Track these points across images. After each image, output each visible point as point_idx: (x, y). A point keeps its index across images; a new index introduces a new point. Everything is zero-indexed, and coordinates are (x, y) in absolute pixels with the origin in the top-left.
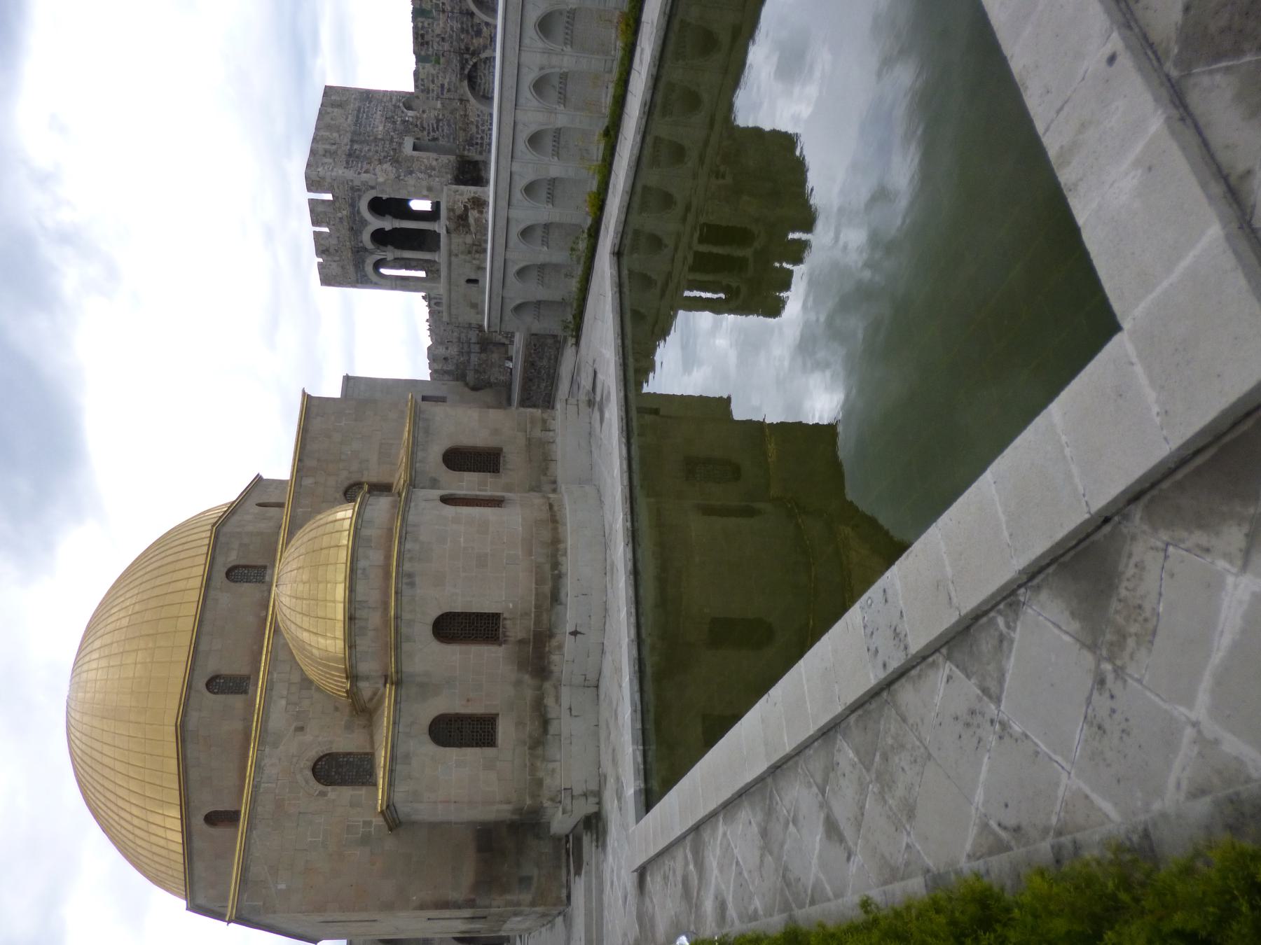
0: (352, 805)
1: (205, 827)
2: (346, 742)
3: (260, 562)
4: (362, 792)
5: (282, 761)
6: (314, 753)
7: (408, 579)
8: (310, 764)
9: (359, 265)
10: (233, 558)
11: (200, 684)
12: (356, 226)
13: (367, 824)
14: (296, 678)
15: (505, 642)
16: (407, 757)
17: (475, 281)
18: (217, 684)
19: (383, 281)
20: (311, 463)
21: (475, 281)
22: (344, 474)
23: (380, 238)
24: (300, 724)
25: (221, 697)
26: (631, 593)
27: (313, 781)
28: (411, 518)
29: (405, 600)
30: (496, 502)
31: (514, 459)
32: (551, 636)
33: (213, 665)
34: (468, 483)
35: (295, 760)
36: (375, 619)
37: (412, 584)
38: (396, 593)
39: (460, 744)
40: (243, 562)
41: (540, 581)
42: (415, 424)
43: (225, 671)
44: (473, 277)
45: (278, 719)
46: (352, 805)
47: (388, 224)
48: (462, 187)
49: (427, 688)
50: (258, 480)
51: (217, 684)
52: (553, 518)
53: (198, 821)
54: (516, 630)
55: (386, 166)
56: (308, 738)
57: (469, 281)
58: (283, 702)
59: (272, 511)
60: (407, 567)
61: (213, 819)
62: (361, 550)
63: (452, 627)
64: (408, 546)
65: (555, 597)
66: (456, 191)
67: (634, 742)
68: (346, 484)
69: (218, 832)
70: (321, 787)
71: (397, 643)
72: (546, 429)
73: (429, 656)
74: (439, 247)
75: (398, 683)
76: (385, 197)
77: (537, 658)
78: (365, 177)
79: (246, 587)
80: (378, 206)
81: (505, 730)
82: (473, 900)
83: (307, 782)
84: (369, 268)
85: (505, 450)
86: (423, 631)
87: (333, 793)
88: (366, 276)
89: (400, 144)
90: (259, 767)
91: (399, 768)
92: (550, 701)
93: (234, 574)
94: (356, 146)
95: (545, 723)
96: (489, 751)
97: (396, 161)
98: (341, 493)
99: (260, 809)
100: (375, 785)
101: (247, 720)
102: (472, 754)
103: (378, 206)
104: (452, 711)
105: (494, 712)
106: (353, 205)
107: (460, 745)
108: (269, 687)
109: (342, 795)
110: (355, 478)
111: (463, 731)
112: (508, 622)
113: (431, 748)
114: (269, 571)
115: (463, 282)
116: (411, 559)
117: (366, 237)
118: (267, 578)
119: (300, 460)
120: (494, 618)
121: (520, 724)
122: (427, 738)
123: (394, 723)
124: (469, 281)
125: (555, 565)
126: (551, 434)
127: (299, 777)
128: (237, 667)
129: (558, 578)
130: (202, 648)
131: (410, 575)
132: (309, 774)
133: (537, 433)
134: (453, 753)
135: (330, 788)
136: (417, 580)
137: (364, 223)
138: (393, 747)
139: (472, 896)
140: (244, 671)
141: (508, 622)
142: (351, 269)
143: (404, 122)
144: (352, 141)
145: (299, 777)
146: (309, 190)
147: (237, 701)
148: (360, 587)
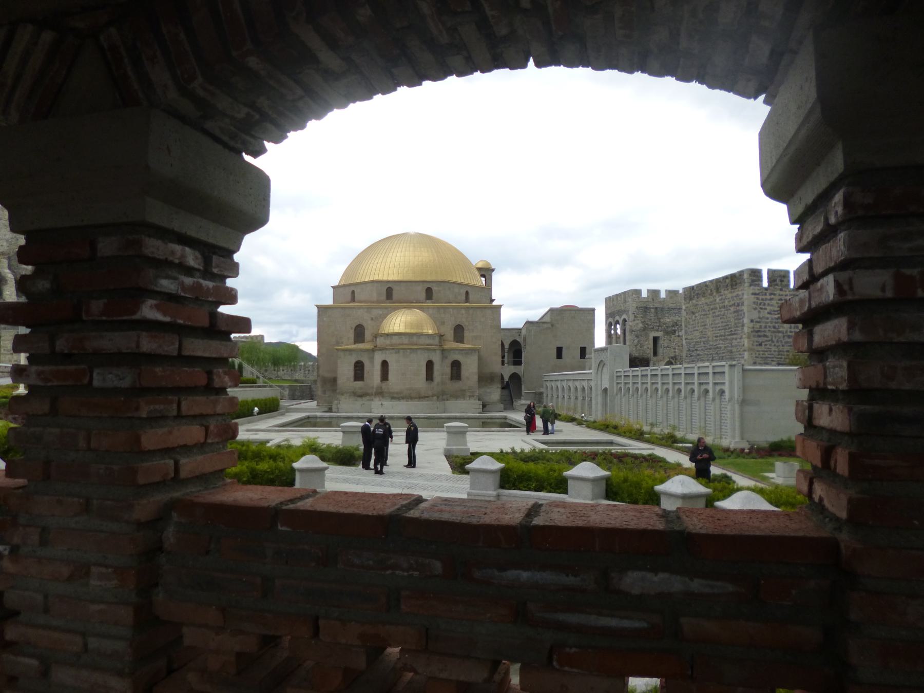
2: (368, 335)
4: (352, 340)
6: (365, 324)
7: (397, 351)
11: (390, 285)
22: (467, 324)
25: (385, 292)
28: (419, 352)
30: (430, 376)
31: (457, 385)
32: (383, 397)
34: (442, 370)
36: (388, 342)
39: (355, 371)
41: (397, 393)
42: (469, 349)
43: (394, 292)
45: (375, 312)
49: (372, 359)
52: (421, 398)
53: (352, 288)
54: (384, 385)
55: (641, 325)
56: (370, 322)
59: (464, 298)
61: (353, 292)
63: (385, 364)
65: (393, 398)
69: (349, 297)
71: (382, 349)
72: (470, 397)
73: (379, 358)
75: (373, 350)
77: (380, 393)
78: (632, 317)
79: (424, 295)
89: (657, 330)
90: (360, 308)
92: (368, 398)
94: (653, 310)
95: (361, 396)
97: (645, 329)
100: (355, 343)
101: (378, 302)
102: (352, 374)
108: (386, 308)
109: (351, 335)
111: (359, 371)
113: (353, 361)
120: (387, 380)
121: (361, 388)
125: (403, 398)
128: (395, 295)
129: (399, 399)
133: (468, 394)
134: (352, 368)
143: (675, 331)
144: (656, 308)
147: (384, 297)
148: (396, 337)
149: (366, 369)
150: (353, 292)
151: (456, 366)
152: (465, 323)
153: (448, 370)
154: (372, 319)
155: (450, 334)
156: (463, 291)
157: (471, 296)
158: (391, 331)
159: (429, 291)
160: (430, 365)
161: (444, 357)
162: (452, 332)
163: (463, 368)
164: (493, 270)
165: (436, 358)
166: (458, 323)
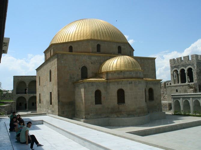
0: (78, 75)
1: (69, 46)
2: (89, 72)
5: (86, 60)
6: (87, 66)
9: (175, 67)
10: (122, 47)
11: (98, 43)
12: (185, 66)
14: (102, 61)
15: (118, 104)
16: (93, 85)
17: (177, 91)
18: (99, 46)
19: (173, 72)
20: (142, 61)
21: (177, 91)
23: (183, 71)
24: (93, 63)
25: (96, 47)
27: (82, 66)
40: (122, 49)
43: (101, 47)
44: (178, 91)
46: (78, 75)
47: (186, 72)
48: (198, 86)
50: (134, 50)
51: (99, 46)
54: (122, 107)
56: (90, 65)
57: (177, 90)
58: (97, 59)
66: (197, 85)
69: (68, 49)
70: (81, 68)
74: (182, 83)
76: (193, 71)
79: (117, 50)
80: (190, 70)
81: (99, 106)
82: (59, 101)
84: (175, 69)
86: (120, 87)
87: (80, 70)
88: (173, 68)
93: (119, 48)
101: (92, 52)
102: (94, 99)
103: (190, 70)
104: (102, 94)
105: (102, 102)
106: (189, 65)
107: (95, 96)
112: (123, 105)
114: (120, 54)
115: (176, 89)
117: (182, 68)
119: (143, 58)
122: (96, 89)
124: (177, 90)
126: (158, 111)
127: (83, 64)
128: (102, 50)
134: (94, 95)
136: (131, 85)
137: (186, 67)
139: (60, 101)
141: (123, 105)
142: (174, 65)
145: (83, 64)
146: (191, 55)
147: (96, 50)
154: (92, 63)
159: (119, 48)
163: (155, 92)
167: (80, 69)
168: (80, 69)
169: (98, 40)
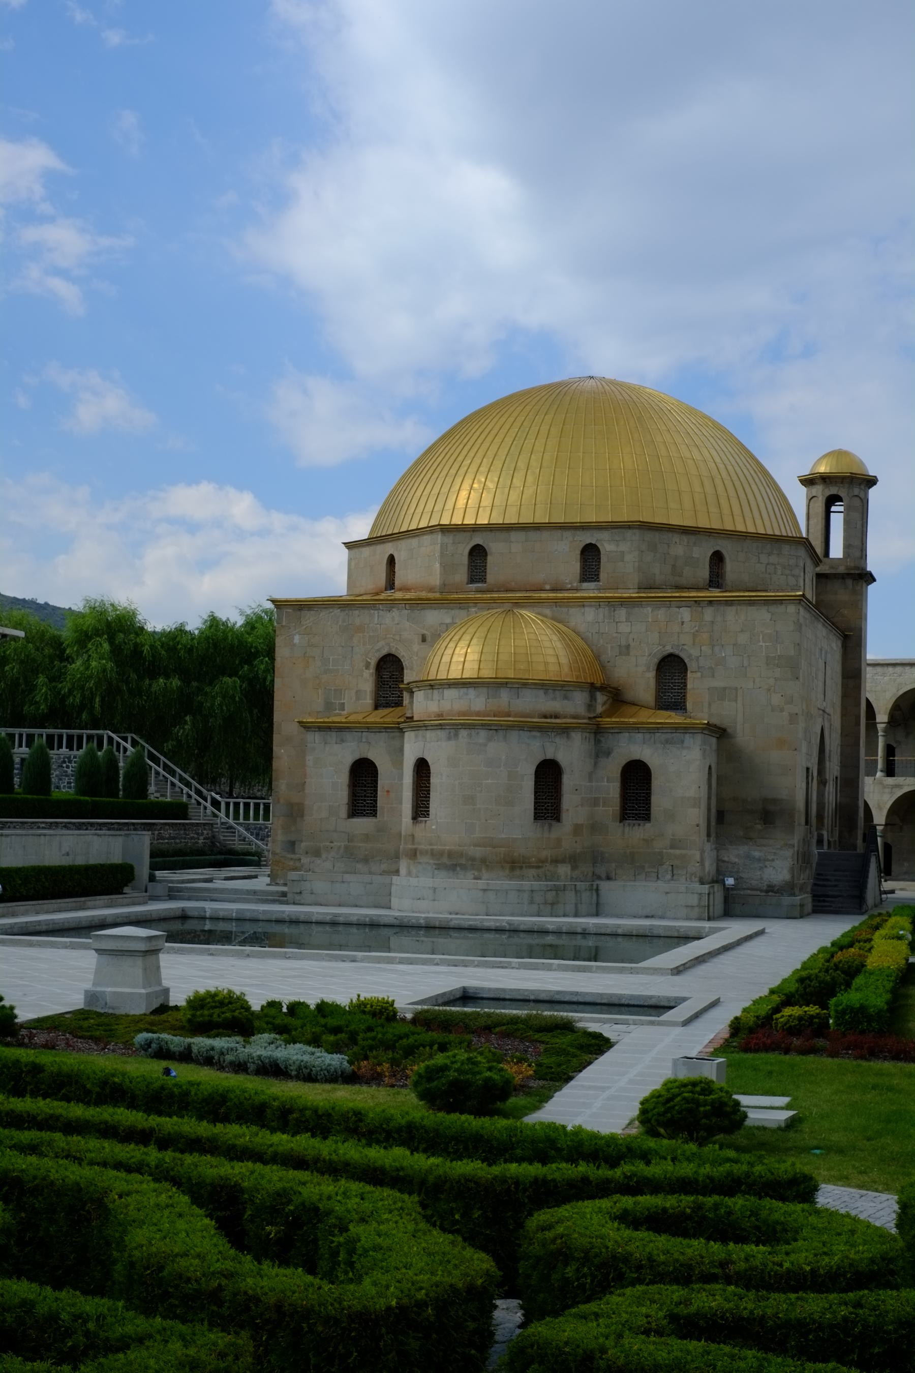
3: (603, 576)
6: (402, 653)
8: (393, 652)
10: (607, 546)
11: (478, 540)
13: (342, 707)
18: (478, 554)
22: (695, 652)
24: (429, 639)
25: (465, 560)
26: (354, 919)
29: (439, 732)
33: (495, 547)
34: (590, 787)
35: (397, 638)
37: (449, 739)
38: (440, 725)
43: (489, 558)
59: (704, 573)
60: (463, 733)
62: (485, 690)
64: (483, 734)
67: (238, 911)
68: (682, 655)
79: (575, 567)
81: (362, 824)
83: (378, 650)
85: (648, 825)
91: (334, 734)
96: (343, 811)
98: (672, 651)
99: (357, 612)
102: (342, 795)
109: (366, 683)
110: (691, 665)
114: (592, 585)
116: (470, 736)
118: (585, 585)
120: (426, 814)
122: (357, 757)
123: (368, 728)
126: (669, 876)
128: (495, 570)
130: (514, 536)
131: (456, 735)
132: (385, 652)
134: (344, 779)
135: (372, 670)
136: (452, 742)
138: (348, 728)
139: (282, 801)
140: (490, 577)
147: (461, 575)
149: (383, 782)
150: (391, 560)
151: (637, 780)
152: (690, 653)
153: (613, 790)
155: (640, 679)
156: (703, 552)
157: (730, 568)
158: (442, 675)
160: (548, 775)
161: (599, 753)
162: (651, 675)
163: (657, 783)
164: (871, 482)
165: (571, 754)
166: (669, 649)
167: (367, 667)
168: (367, 667)
169: (475, 529)
